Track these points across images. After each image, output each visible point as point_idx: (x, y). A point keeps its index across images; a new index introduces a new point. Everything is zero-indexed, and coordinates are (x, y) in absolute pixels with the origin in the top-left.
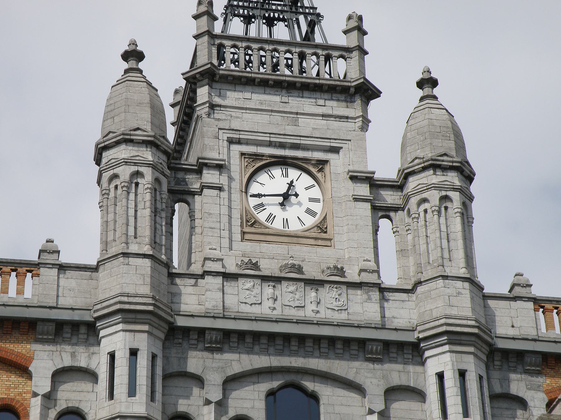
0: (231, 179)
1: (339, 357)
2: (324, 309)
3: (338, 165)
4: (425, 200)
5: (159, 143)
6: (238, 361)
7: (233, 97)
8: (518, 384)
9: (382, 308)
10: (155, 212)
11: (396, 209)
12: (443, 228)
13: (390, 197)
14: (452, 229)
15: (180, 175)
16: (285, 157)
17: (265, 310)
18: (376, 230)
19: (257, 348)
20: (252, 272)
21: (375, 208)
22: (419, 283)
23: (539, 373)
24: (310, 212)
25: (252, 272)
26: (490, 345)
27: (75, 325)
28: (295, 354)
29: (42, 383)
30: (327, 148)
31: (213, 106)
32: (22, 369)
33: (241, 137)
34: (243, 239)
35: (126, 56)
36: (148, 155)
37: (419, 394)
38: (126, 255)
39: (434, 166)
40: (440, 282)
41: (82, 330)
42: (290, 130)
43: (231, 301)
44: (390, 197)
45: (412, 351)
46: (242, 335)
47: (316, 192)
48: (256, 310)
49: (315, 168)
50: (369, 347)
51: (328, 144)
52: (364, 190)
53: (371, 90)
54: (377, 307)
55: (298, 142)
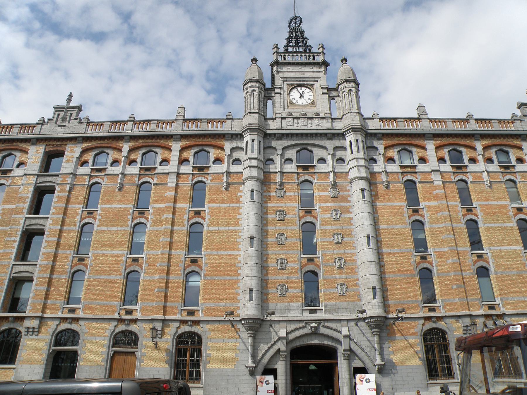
0: (284, 91)
1: (319, 139)
2: (314, 126)
3: (317, 85)
4: (344, 92)
6: (287, 143)
7: (285, 69)
8: (376, 144)
9: (332, 124)
10: (260, 101)
11: (336, 96)
12: (350, 99)
13: (334, 93)
14: (353, 99)
15: (269, 92)
17: (295, 127)
18: (330, 103)
19: (293, 138)
20: (291, 116)
21: (329, 97)
22: (343, 115)
23: (381, 139)
24: (309, 99)
25: (291, 116)
26: (366, 132)
27: (237, 135)
28: (305, 139)
29: (227, 151)
31: (278, 72)
32: (222, 148)
35: (252, 61)
36: (257, 85)
37: (344, 148)
38: (250, 113)
39: (346, 81)
40: (350, 114)
41: (239, 136)
42: (302, 76)
43: (284, 125)
44: (334, 93)
45: (342, 136)
46: (287, 134)
47: (311, 93)
48: (292, 127)
49: (310, 87)
50: (328, 135)
52: (326, 91)
54: (330, 124)
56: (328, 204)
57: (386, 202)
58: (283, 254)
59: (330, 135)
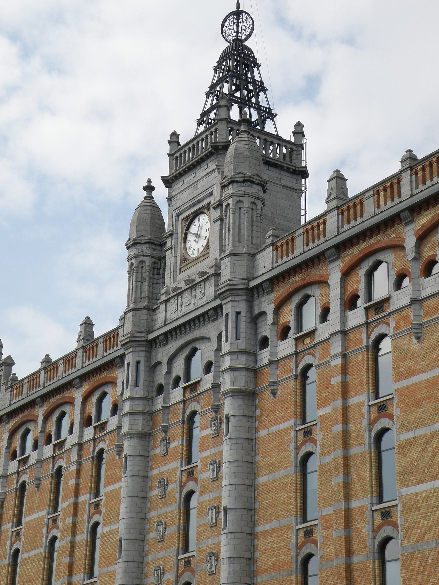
5: (139, 241)
16: (196, 211)
30: (209, 195)
33: (180, 210)
34: (180, 272)
42: (196, 193)
51: (208, 192)
53: (220, 145)
55: (198, 199)
56: (208, 453)
57: (271, 426)
58: (162, 558)
59: (211, 313)
